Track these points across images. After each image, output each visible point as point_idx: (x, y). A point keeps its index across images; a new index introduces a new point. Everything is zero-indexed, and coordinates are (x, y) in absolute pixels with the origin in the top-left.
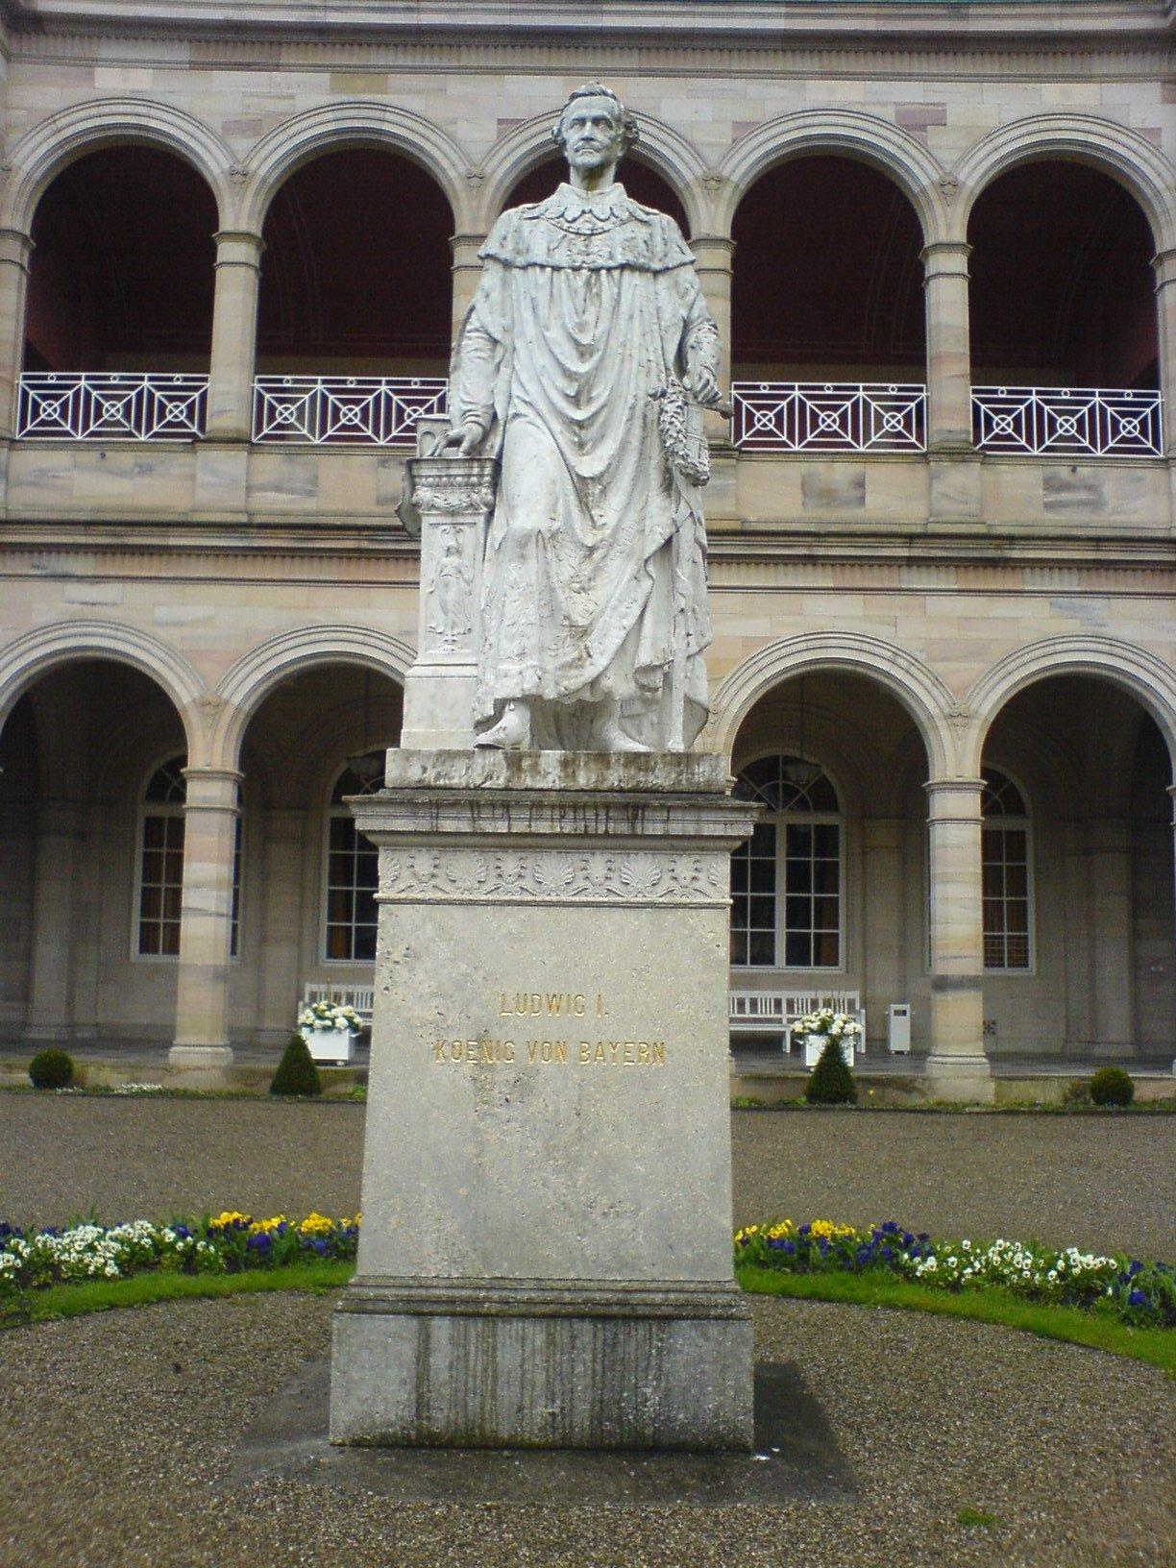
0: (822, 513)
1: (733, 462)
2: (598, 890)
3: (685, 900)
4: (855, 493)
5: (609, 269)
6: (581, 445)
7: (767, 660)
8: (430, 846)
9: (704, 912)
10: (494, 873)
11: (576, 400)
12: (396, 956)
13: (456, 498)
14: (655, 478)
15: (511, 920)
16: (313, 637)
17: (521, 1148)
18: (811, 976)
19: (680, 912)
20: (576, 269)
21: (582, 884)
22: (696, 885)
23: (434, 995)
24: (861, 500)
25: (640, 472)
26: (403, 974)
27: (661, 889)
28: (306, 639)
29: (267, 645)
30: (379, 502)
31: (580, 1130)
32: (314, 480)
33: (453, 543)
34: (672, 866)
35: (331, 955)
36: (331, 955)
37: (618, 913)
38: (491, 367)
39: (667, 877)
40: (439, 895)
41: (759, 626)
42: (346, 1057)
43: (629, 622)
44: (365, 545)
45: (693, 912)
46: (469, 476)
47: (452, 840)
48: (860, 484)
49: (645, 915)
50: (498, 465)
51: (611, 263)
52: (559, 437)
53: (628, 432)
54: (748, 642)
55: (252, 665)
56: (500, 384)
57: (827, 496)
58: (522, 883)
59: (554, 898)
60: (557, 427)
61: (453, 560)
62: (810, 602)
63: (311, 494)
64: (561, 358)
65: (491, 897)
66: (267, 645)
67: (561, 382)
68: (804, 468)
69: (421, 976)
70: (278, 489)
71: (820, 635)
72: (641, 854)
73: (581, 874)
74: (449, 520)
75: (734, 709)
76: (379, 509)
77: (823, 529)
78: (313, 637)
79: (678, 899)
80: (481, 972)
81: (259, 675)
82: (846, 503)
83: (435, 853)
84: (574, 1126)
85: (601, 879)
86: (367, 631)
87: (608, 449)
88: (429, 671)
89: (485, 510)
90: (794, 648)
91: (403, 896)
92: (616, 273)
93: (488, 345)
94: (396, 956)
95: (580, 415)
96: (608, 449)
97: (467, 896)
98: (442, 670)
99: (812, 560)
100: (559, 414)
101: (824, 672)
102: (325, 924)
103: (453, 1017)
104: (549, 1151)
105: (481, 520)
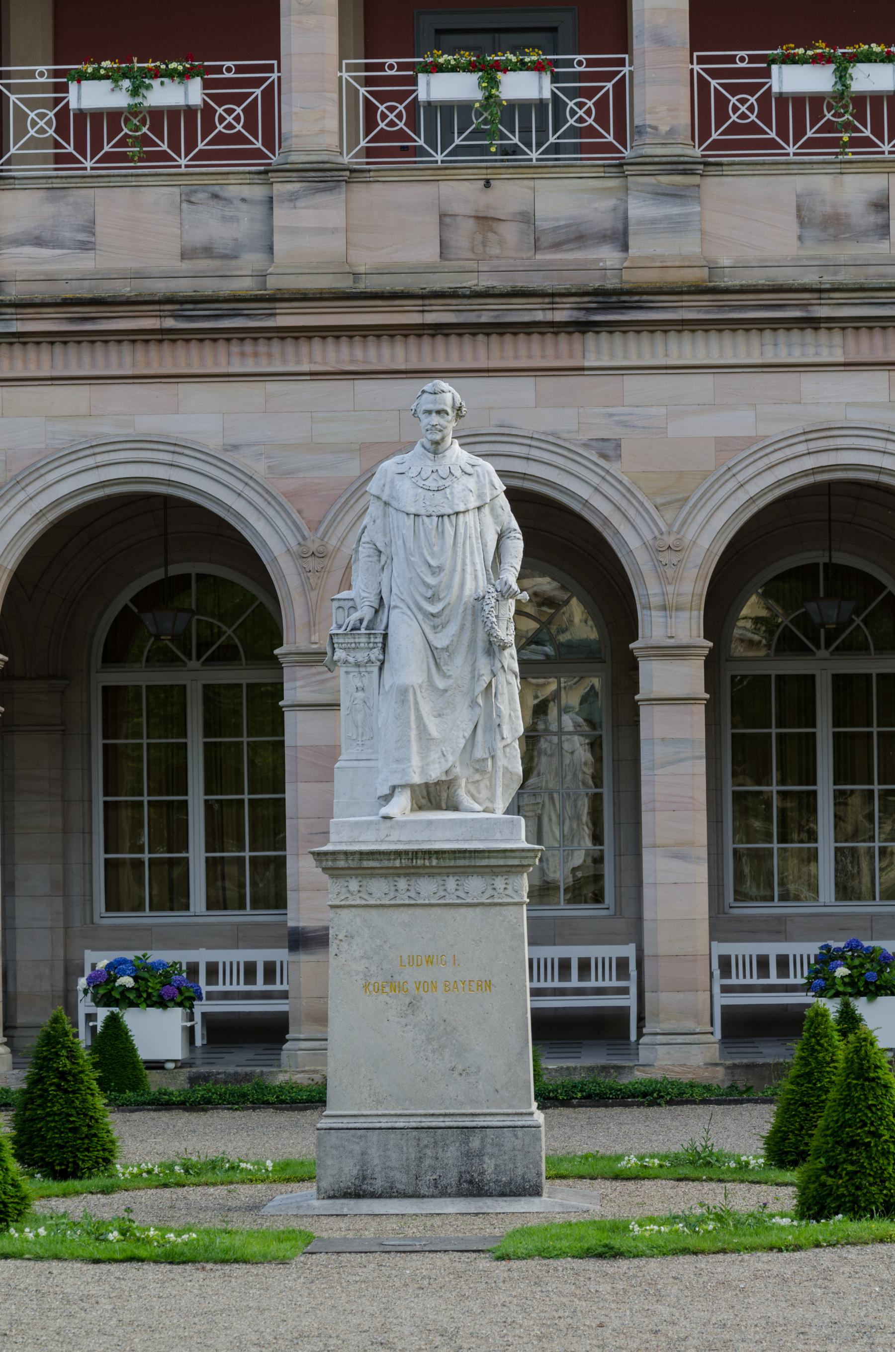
0: (829, 251)
1: (696, 180)
2: (452, 896)
3: (500, 901)
4: (873, 219)
5: (449, 516)
6: (434, 627)
7: (752, 470)
8: (357, 876)
9: (511, 908)
10: (393, 888)
11: (432, 599)
12: (340, 937)
13: (361, 656)
14: (481, 644)
15: (404, 915)
16: (100, 459)
17: (414, 1040)
18: (873, 917)
19: (498, 908)
20: (429, 516)
21: (443, 894)
22: (506, 892)
23: (362, 957)
24: (884, 230)
25: (473, 641)
26: (345, 946)
27: (487, 895)
28: (90, 462)
29: (35, 471)
30: (185, 255)
31: (445, 1029)
32: (90, 228)
33: (360, 684)
34: (493, 882)
35: (113, 904)
36: (113, 904)
37: (463, 910)
38: (378, 567)
39: (490, 888)
40: (364, 902)
41: (738, 423)
42: (179, 1056)
43: (468, 734)
44: (170, 323)
45: (505, 908)
46: (369, 643)
47: (369, 872)
48: (881, 206)
49: (478, 909)
50: (385, 636)
51: (451, 512)
52: (422, 623)
53: (464, 619)
54: (723, 444)
55: (15, 503)
56: (385, 576)
57: (834, 225)
58: (409, 894)
59: (427, 902)
60: (420, 617)
61: (360, 694)
62: (809, 383)
63: (85, 246)
64: (422, 575)
65: (392, 902)
66: (35, 471)
67: (422, 589)
68: (800, 183)
69: (355, 947)
70: (38, 241)
71: (826, 431)
72: (475, 876)
73: (442, 888)
74: (357, 670)
75: (705, 542)
76: (186, 266)
77: (828, 279)
78: (100, 459)
79: (496, 900)
80: (388, 944)
81: (23, 517)
82: (859, 235)
83: (360, 879)
84: (442, 1027)
85: (453, 891)
86: (176, 446)
87: (452, 629)
88: (350, 764)
89: (379, 664)
90: (789, 452)
91: (343, 903)
92: (453, 518)
93: (377, 553)
94: (340, 937)
95: (434, 609)
96: (452, 629)
97: (378, 902)
98: (356, 763)
99: (813, 323)
100: (420, 608)
101: (830, 484)
102: (100, 856)
103: (373, 969)
104: (429, 1040)
105: (376, 670)
